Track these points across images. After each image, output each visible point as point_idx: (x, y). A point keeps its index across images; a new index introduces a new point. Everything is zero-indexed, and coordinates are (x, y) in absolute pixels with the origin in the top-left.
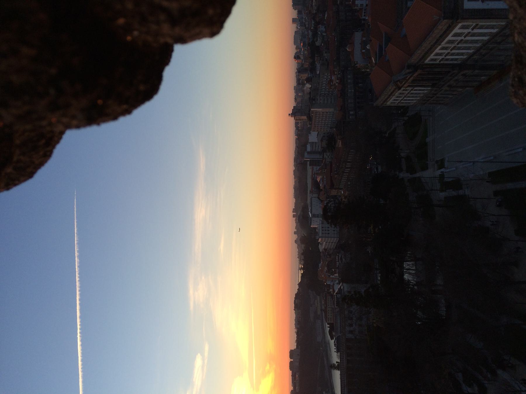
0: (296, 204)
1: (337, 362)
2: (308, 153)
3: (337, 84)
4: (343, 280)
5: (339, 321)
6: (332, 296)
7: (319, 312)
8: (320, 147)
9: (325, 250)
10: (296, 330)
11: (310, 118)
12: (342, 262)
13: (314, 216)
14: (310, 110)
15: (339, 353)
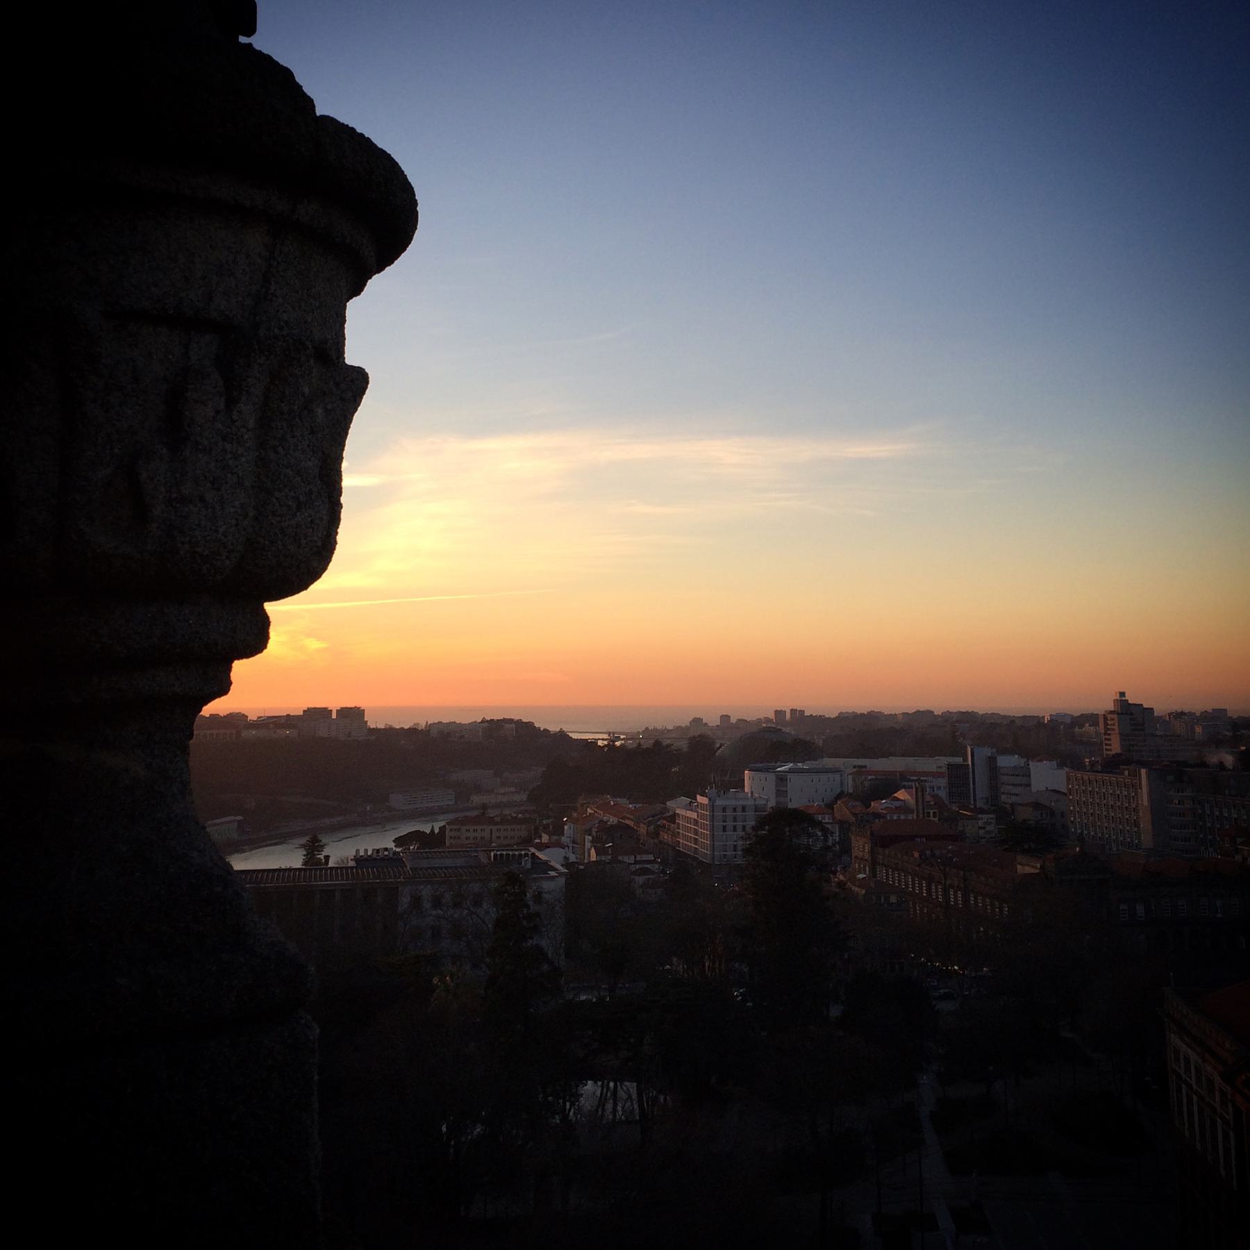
0: (820, 720)
1: (327, 858)
2: (992, 760)
3: (1238, 858)
4: (575, 874)
5: (448, 862)
6: (527, 841)
7: (477, 799)
8: (1014, 799)
9: (673, 818)
10: (422, 725)
11: (1112, 765)
12: (636, 873)
13: (782, 779)
14: (1142, 764)
15: (352, 864)
